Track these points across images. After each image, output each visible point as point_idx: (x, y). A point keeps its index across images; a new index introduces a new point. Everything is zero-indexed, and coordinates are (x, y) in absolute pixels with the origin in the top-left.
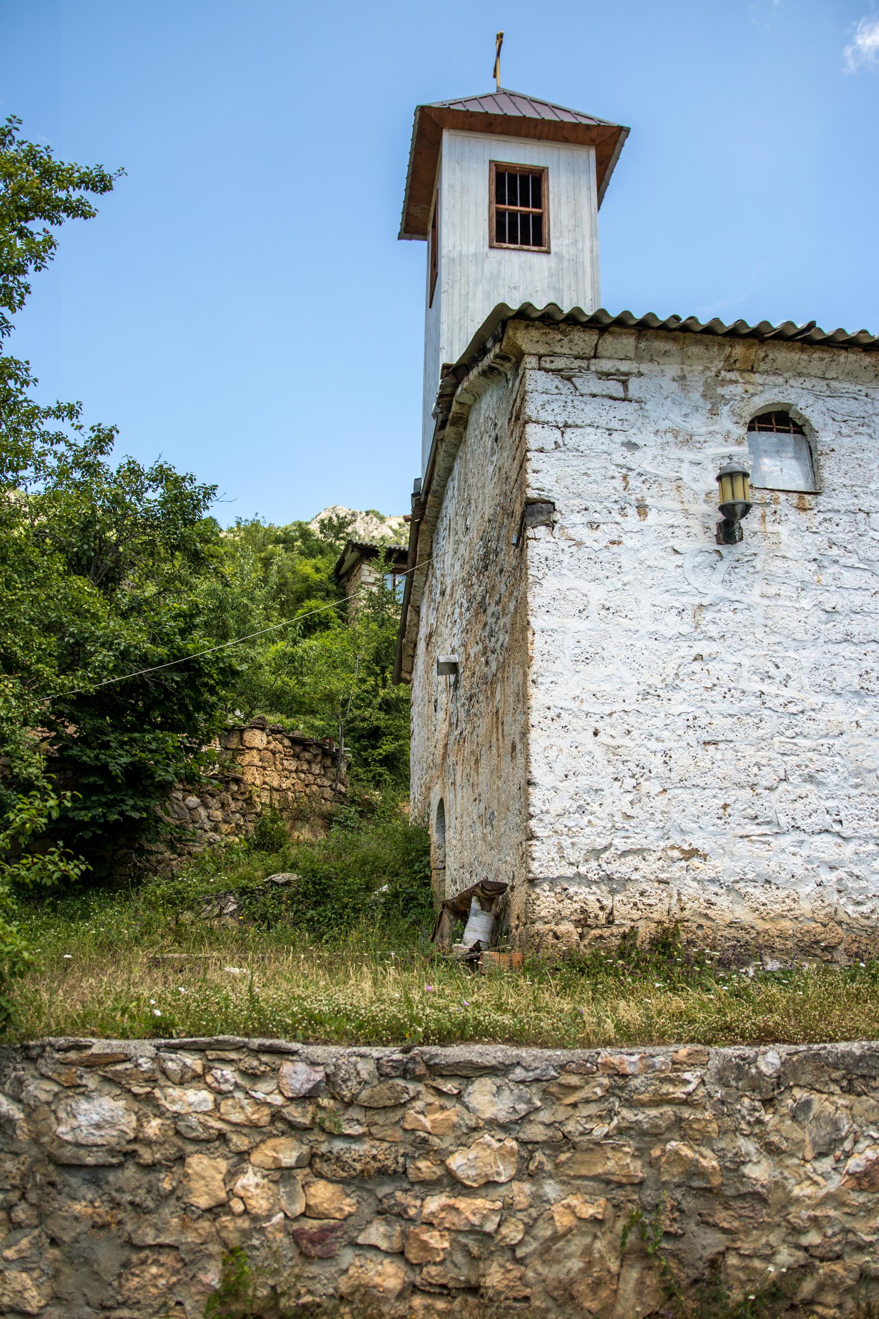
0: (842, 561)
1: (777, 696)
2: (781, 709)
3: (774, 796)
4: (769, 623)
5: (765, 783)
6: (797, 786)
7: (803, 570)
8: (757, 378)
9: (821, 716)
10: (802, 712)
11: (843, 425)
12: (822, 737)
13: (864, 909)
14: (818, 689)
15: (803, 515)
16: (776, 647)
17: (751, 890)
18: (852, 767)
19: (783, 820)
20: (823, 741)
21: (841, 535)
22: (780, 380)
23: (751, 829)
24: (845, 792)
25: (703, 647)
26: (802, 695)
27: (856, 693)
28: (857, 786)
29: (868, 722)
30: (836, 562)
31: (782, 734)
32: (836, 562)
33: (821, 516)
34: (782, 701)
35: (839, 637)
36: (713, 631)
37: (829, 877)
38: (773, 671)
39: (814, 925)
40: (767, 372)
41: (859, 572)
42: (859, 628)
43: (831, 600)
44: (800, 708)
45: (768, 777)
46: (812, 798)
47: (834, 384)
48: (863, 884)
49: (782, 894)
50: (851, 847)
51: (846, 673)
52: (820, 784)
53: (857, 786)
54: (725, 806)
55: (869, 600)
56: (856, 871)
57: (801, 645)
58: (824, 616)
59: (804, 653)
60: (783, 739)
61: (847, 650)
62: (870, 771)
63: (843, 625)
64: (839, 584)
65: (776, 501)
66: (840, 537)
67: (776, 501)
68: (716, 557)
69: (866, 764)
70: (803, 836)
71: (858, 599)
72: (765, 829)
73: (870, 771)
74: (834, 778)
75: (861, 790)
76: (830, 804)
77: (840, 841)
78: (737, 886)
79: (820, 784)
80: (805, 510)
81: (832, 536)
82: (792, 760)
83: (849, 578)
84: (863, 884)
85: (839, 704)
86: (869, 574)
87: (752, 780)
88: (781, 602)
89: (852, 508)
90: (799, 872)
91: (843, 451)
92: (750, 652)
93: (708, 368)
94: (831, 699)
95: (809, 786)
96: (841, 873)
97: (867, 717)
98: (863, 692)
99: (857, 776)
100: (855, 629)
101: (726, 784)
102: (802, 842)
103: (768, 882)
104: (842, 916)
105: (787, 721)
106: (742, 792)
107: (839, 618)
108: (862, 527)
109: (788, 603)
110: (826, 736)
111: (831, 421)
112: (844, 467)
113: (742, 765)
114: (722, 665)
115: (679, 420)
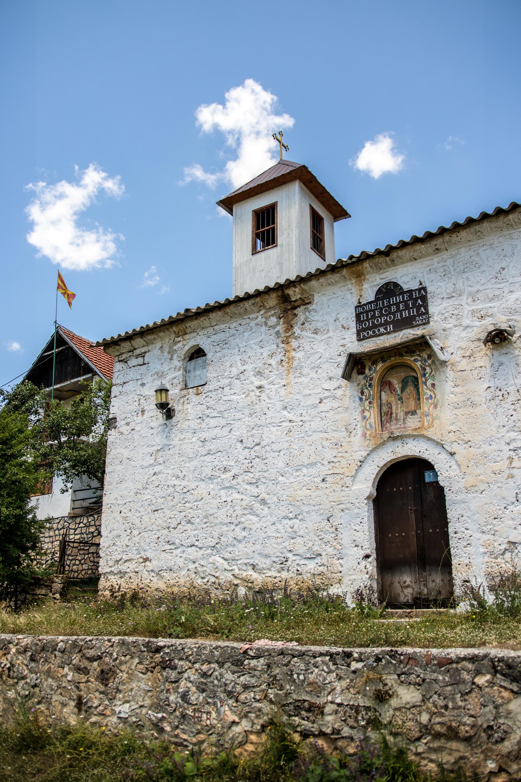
0: (210, 415)
1: (180, 485)
2: (181, 491)
3: (176, 531)
4: (181, 452)
5: (172, 526)
6: (184, 526)
7: (194, 424)
8: (187, 337)
9: (195, 492)
10: (188, 491)
11: (217, 347)
12: (195, 502)
13: (205, 580)
14: (196, 479)
15: (198, 397)
16: (182, 463)
17: (165, 574)
18: (204, 514)
19: (177, 541)
20: (195, 503)
21: (212, 402)
22: (195, 334)
23: (168, 547)
24: (201, 526)
25: (157, 469)
26: (189, 484)
27: (209, 478)
28: (206, 523)
29: (213, 492)
30: (208, 416)
31: (180, 502)
32: (208, 416)
33: (205, 395)
34: (181, 487)
35: (205, 453)
36: (161, 460)
37: (192, 566)
38: (180, 474)
39: (185, 589)
40: (191, 332)
41: (217, 418)
42: (214, 446)
43: (204, 435)
44: (187, 490)
45: (174, 524)
46: (189, 531)
47: (216, 327)
48: (205, 569)
49: (175, 575)
50: (202, 551)
51: (206, 470)
52: (192, 524)
53: (206, 523)
54: (158, 538)
55: (219, 431)
56: (202, 563)
57: (191, 459)
58: (201, 444)
59: (192, 463)
60: (181, 505)
61: (209, 458)
62: (211, 515)
63: (209, 446)
64: (208, 426)
65: (188, 394)
66: (212, 403)
67: (188, 394)
68: (165, 426)
69: (210, 512)
70: (185, 549)
71: (214, 432)
72: (172, 547)
73: (211, 515)
74: (198, 520)
75: (208, 524)
76: (195, 532)
77: (198, 549)
78: (160, 573)
79: (192, 524)
80: (198, 394)
81: (208, 404)
82: (183, 514)
83: (213, 422)
84: (205, 569)
85: (202, 485)
86: (221, 418)
87: (168, 525)
88: (185, 441)
89: (216, 388)
90: (181, 565)
91: (216, 360)
92: (172, 467)
93: (170, 339)
94: (200, 483)
95: (189, 525)
96: (197, 565)
97: (213, 489)
98: (212, 477)
99: (206, 517)
100: (212, 447)
101: (160, 528)
102: (184, 551)
103: (171, 570)
104: (195, 584)
105: (182, 496)
106: (164, 531)
107: (207, 443)
108: (220, 396)
109: (188, 441)
110: (196, 501)
111: (212, 347)
112: (216, 368)
113: (165, 519)
114: (162, 475)
115: (159, 367)
